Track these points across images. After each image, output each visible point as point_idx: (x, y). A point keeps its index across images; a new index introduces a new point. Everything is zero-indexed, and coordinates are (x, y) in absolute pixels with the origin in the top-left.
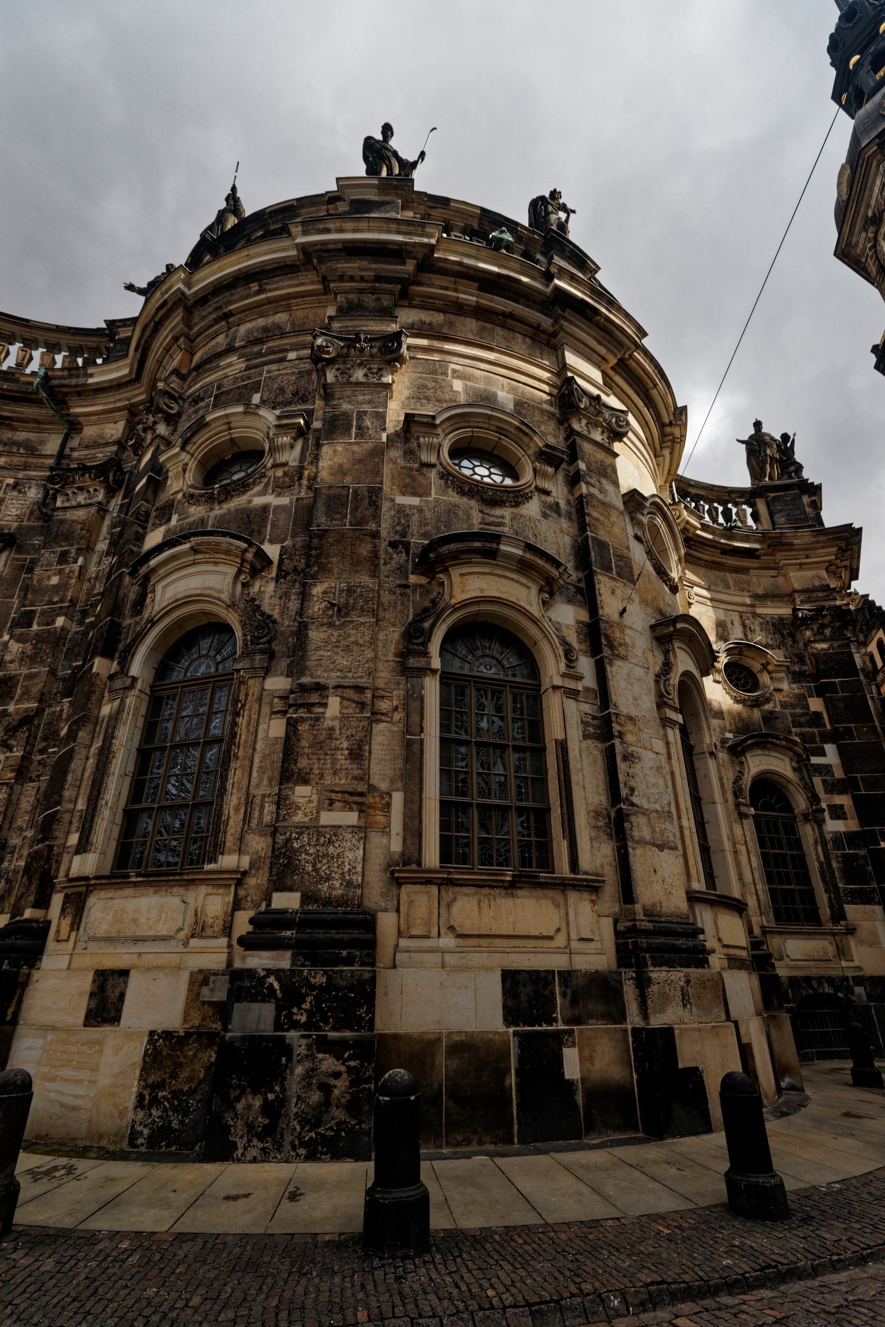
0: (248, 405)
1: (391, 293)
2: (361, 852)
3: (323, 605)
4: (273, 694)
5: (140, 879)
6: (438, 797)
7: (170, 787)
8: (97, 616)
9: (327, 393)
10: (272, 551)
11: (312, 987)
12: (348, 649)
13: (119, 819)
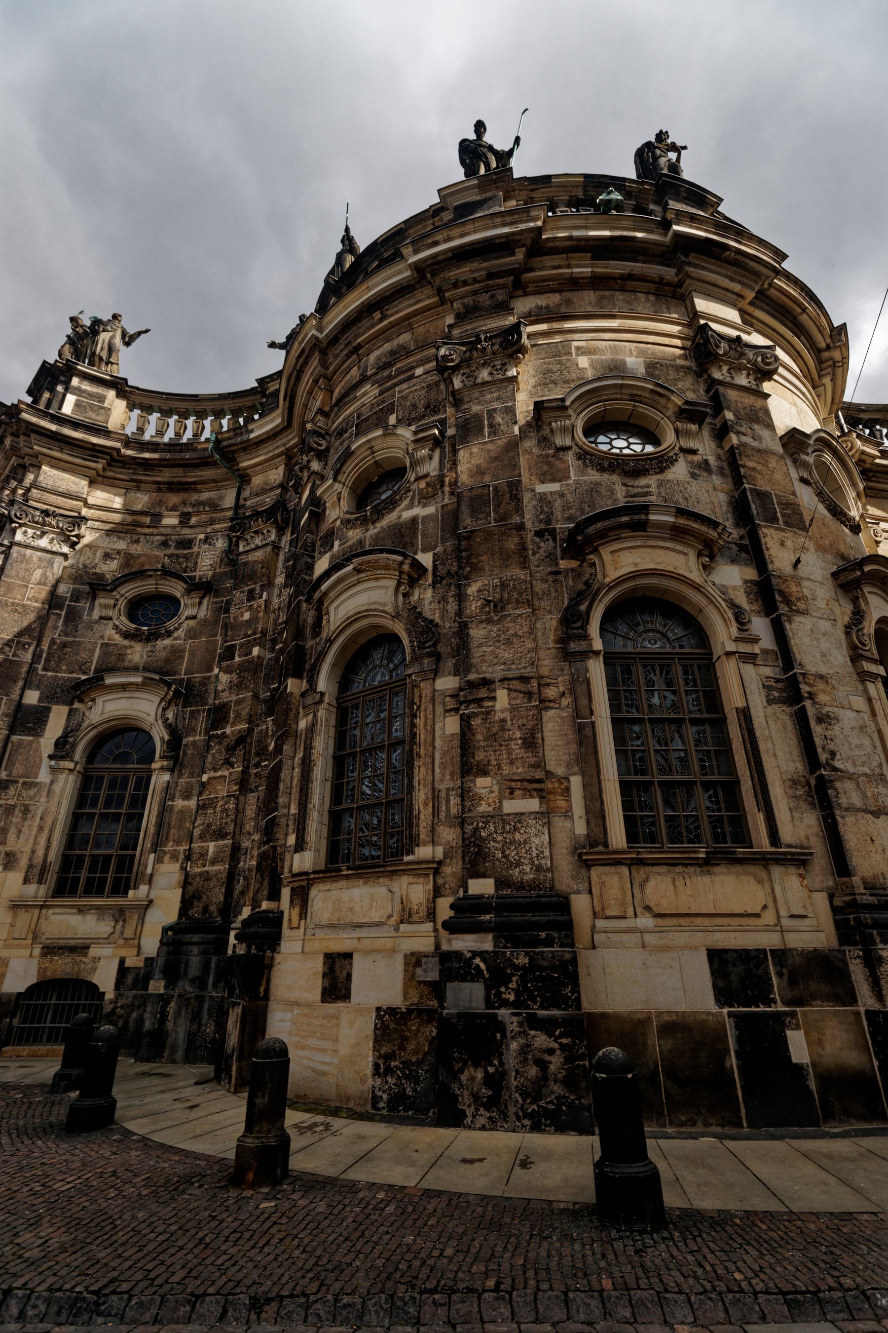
0: (386, 427)
1: (504, 286)
2: (547, 837)
3: (479, 603)
4: (444, 694)
5: (350, 872)
6: (617, 778)
7: (364, 788)
8: (285, 643)
10: (426, 559)
11: (516, 968)
12: (508, 642)
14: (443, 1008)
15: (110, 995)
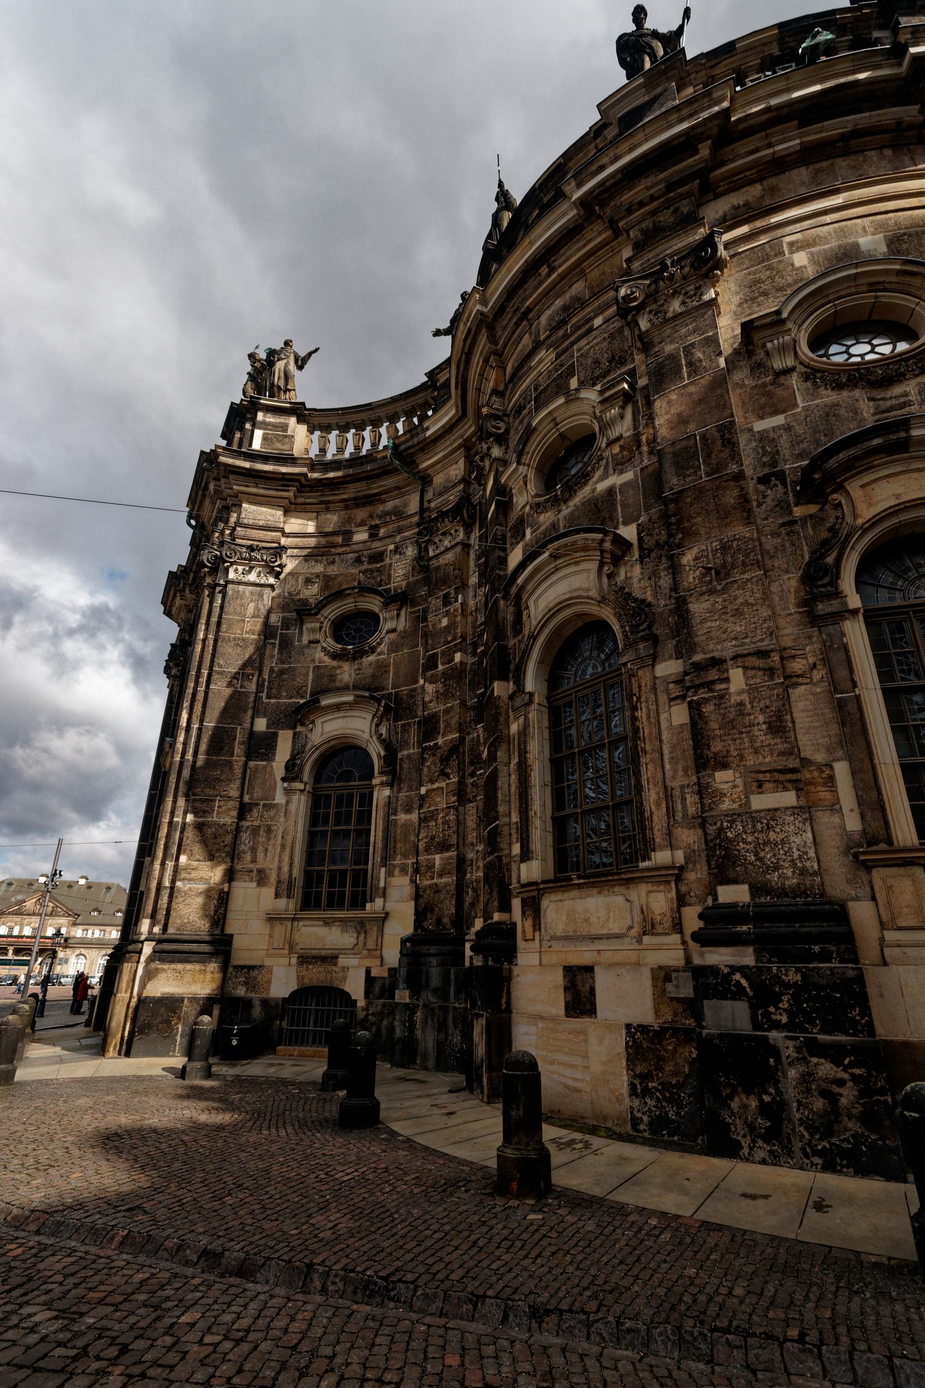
0: (567, 392)
1: (689, 194)
2: (810, 835)
3: (698, 573)
4: (666, 680)
5: (582, 881)
6: (896, 760)
7: (587, 790)
8: (486, 645)
10: (629, 532)
11: (787, 986)
12: (738, 613)
13: (550, 828)
14: (702, 1027)
15: (361, 1003)
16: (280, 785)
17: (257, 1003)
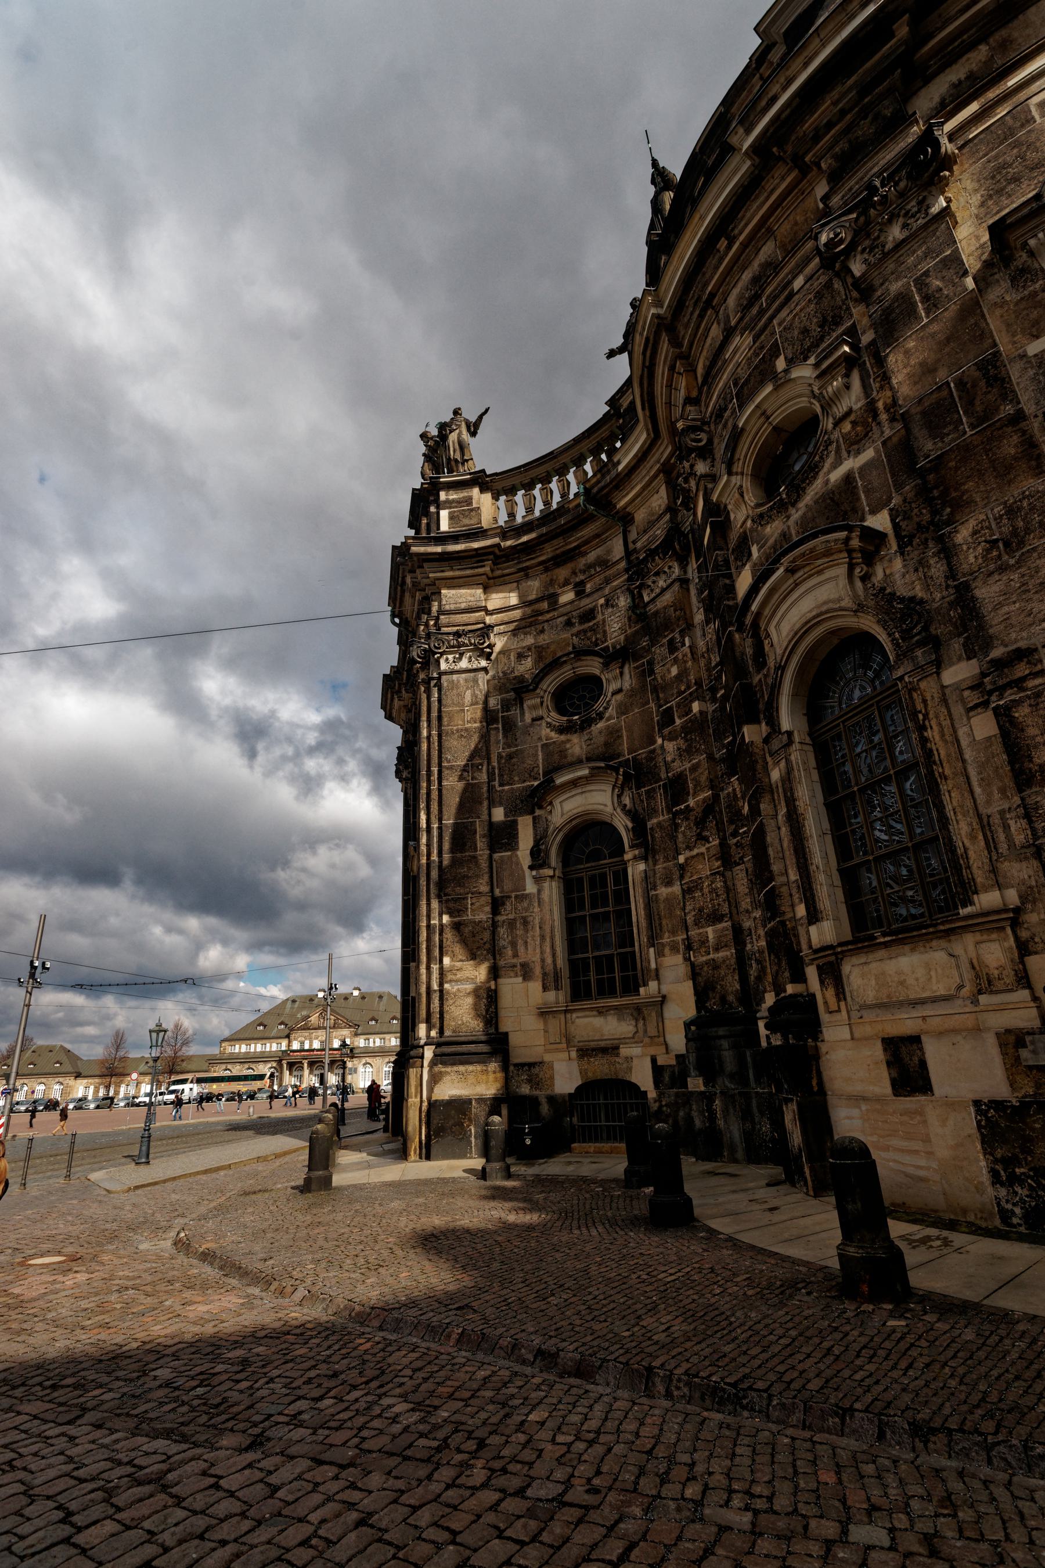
3: (980, 550)
4: (957, 687)
7: (877, 833)
8: (725, 687)
9: (864, 290)
10: (880, 522)
13: (838, 882)
15: (652, 1094)
16: (529, 875)
17: (543, 1101)
